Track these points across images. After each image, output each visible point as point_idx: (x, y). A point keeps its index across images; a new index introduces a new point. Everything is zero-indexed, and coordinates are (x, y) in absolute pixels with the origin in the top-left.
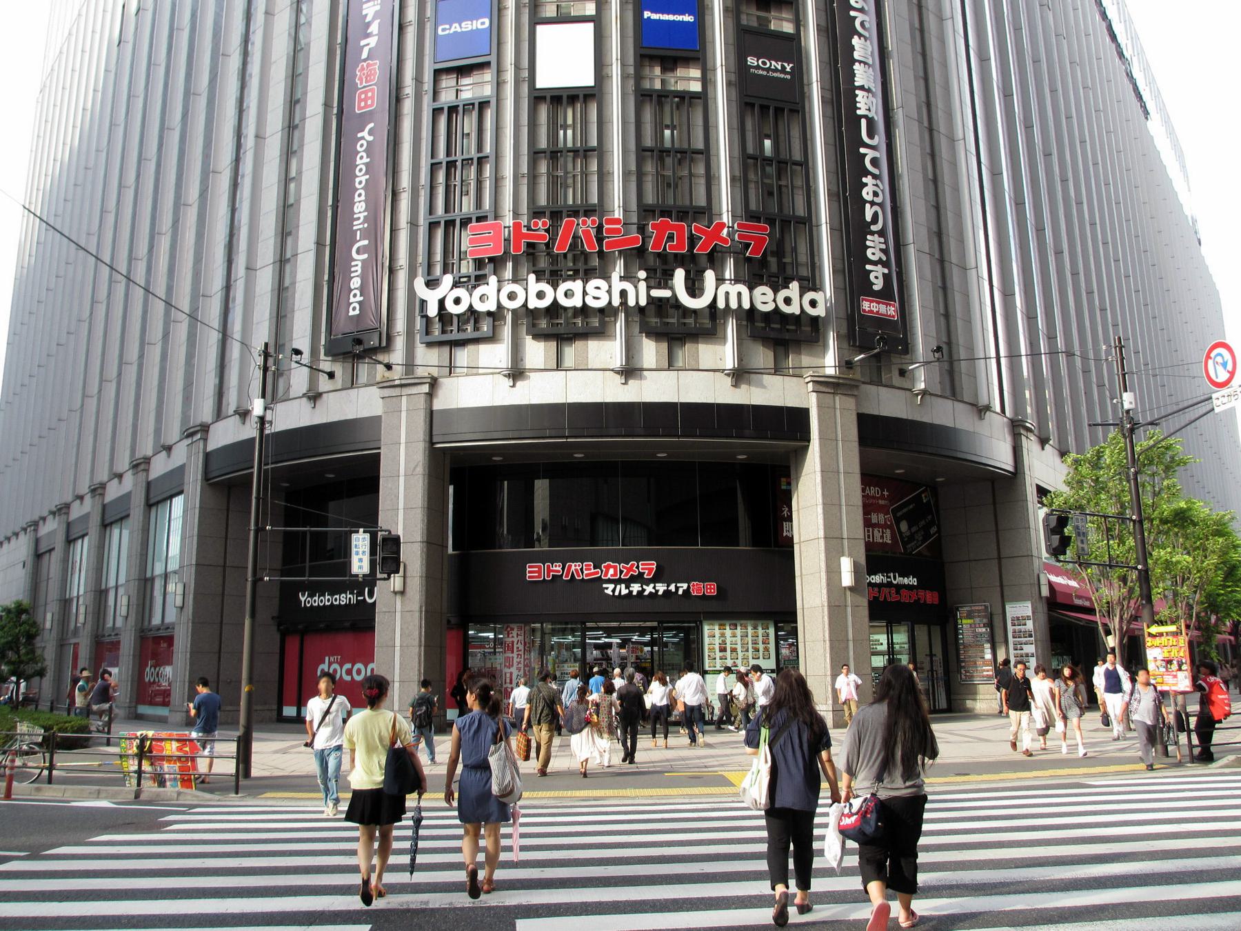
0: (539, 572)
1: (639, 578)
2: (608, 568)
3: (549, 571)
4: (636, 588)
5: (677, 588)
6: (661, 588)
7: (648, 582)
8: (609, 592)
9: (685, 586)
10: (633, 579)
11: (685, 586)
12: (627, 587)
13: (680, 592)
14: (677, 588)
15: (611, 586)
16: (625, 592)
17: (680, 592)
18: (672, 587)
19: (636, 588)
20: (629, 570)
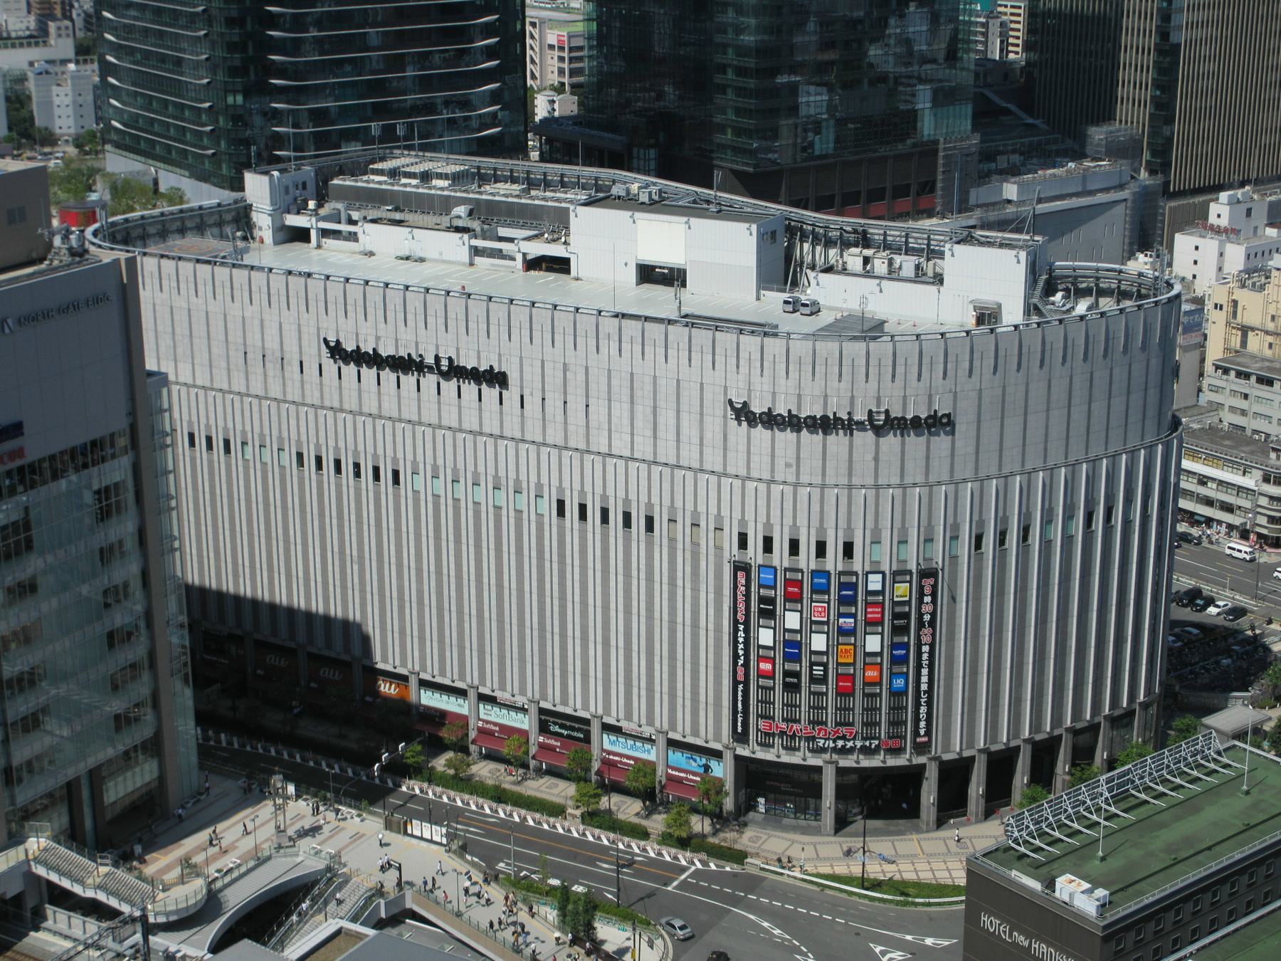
0: (770, 727)
1: (843, 738)
2: (820, 730)
3: (777, 727)
4: (840, 743)
5: (871, 744)
6: (859, 744)
7: (849, 740)
8: (821, 744)
9: (877, 742)
10: (839, 738)
11: (877, 742)
12: (834, 741)
13: (873, 746)
14: (871, 744)
15: (823, 741)
16: (832, 745)
17: (873, 746)
18: (867, 743)
19: (840, 743)
20: (837, 732)
